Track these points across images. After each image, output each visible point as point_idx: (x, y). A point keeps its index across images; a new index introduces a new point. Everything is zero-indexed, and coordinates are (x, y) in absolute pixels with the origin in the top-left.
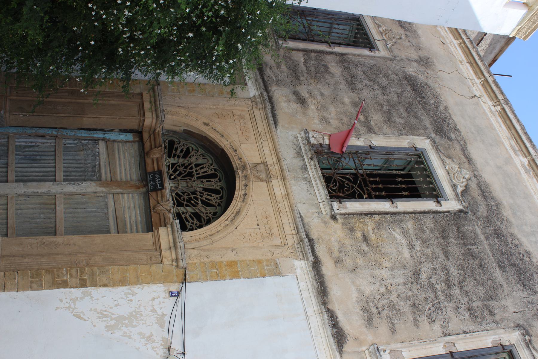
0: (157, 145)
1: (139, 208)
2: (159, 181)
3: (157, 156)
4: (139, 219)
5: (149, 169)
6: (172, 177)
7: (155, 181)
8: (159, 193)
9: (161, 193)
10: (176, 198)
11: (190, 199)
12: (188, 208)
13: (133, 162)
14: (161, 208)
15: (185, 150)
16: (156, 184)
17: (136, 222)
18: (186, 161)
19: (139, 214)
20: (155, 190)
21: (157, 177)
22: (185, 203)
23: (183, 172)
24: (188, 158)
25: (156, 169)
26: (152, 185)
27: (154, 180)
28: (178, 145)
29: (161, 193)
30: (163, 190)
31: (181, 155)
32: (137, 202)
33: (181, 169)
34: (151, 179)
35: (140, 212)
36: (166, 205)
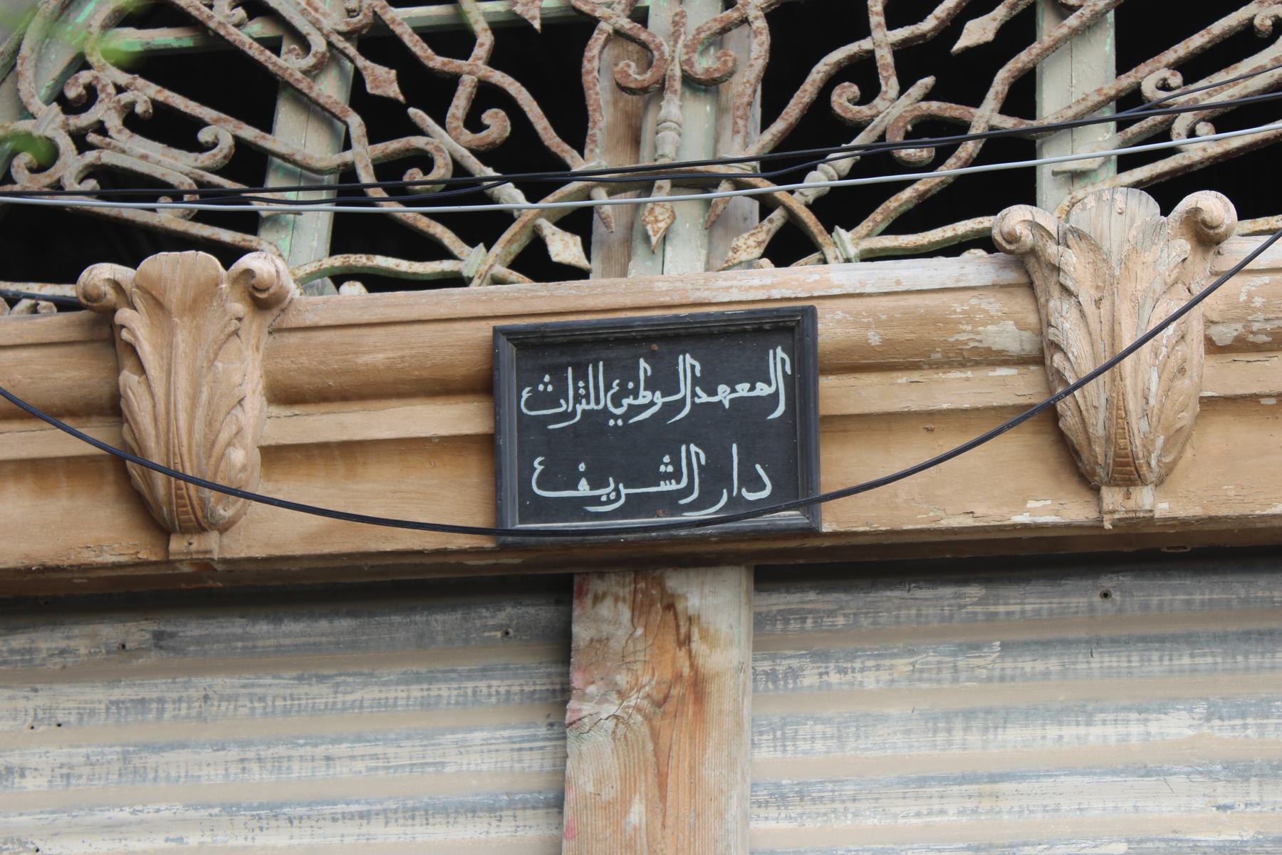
0: (68, 374)
1: (999, 717)
2: (665, 381)
3: (246, 370)
4: (1176, 727)
5: (441, 506)
6: (564, 248)
7: (661, 436)
8: (836, 393)
9: (857, 363)
10: (900, 225)
11: (911, 61)
12: (1053, 102)
13: (212, 771)
14: (1143, 374)
15: (145, 93)
16: (707, 426)
17: (1239, 770)
18: (331, 90)
19: (1102, 734)
20: (793, 443)
21: (590, 396)
22: (987, 116)
23: (497, 124)
24: (290, 63)
25: (459, 418)
26: (715, 477)
27: (627, 451)
28: (71, 164)
29: (857, 363)
30: (832, 328)
31: (222, 131)
32: (896, 742)
33: (446, 142)
34: (614, 494)
35: (1059, 715)
36: (1107, 287)
